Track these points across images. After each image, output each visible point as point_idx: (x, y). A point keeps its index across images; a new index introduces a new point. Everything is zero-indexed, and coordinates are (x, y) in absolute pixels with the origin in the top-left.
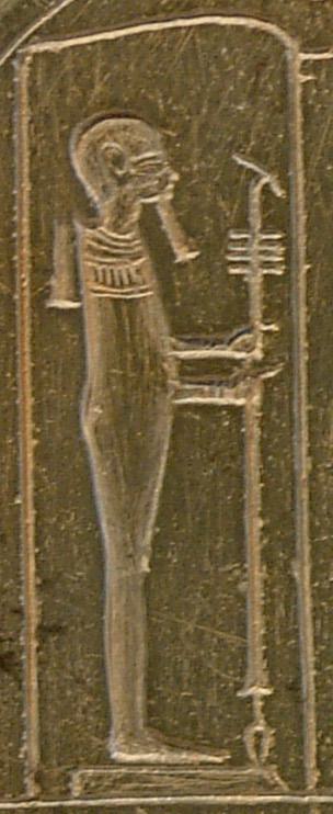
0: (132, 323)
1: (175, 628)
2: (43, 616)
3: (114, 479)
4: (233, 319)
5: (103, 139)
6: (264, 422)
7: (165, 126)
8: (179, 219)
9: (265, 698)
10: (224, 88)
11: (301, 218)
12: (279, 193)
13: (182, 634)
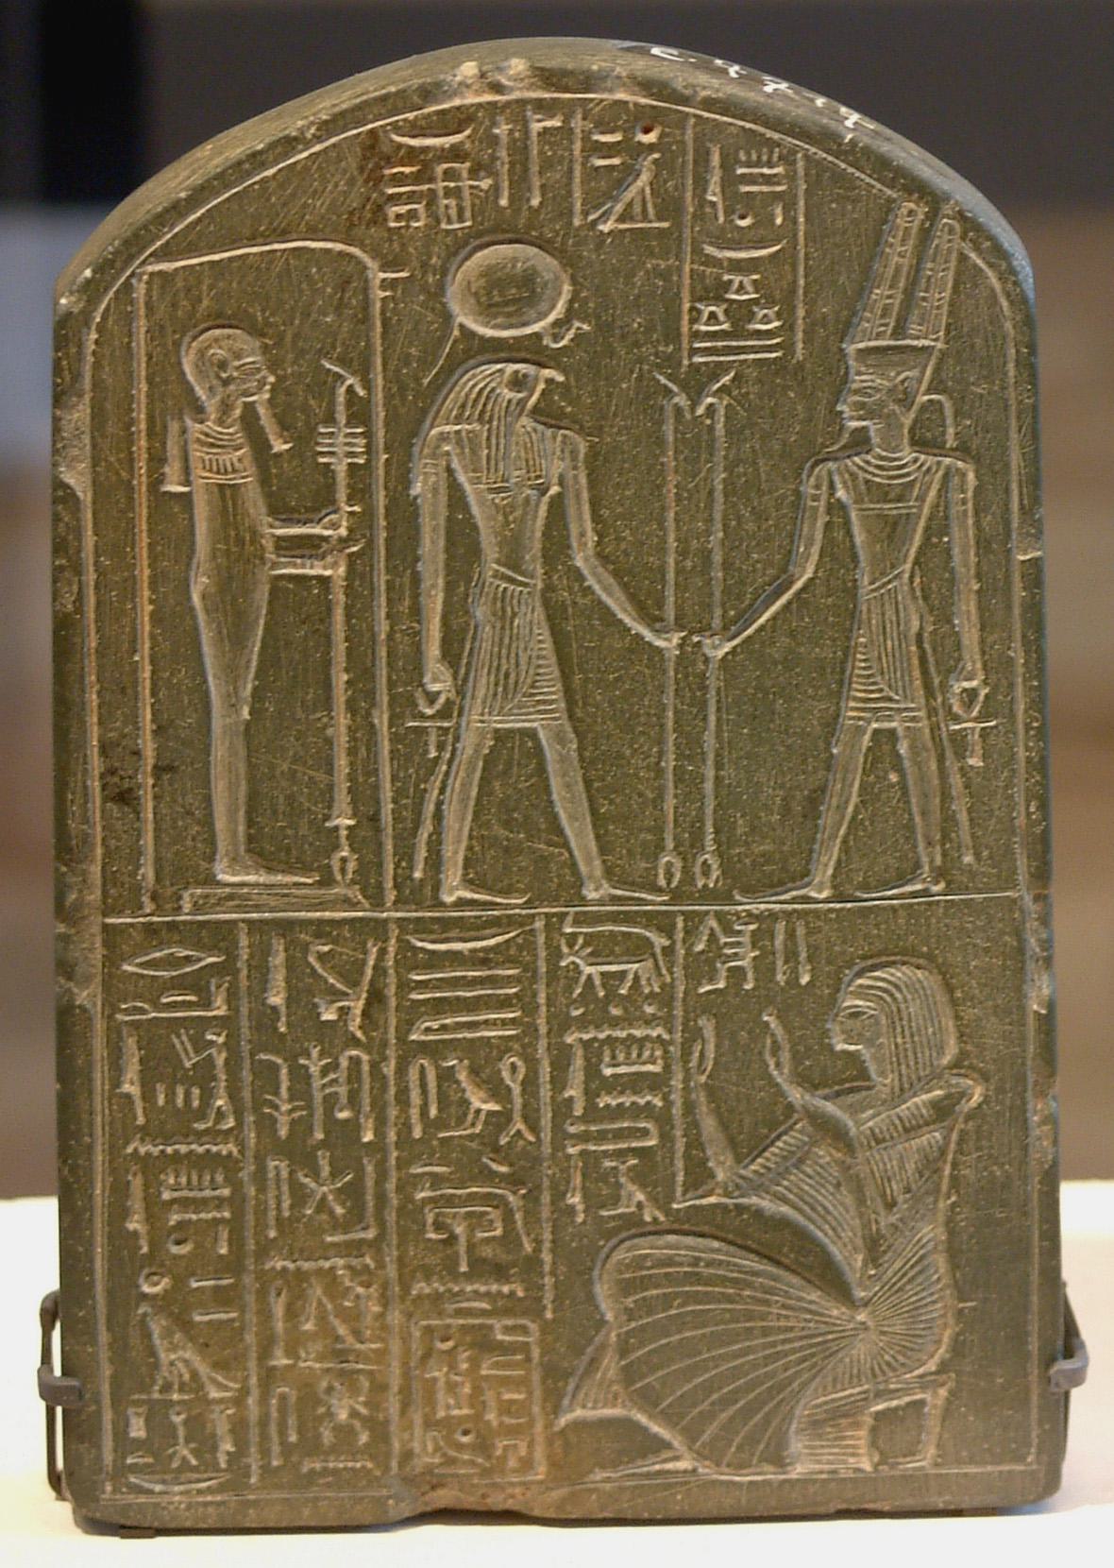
0: (235, 505)
1: (272, 767)
2: (158, 757)
3: (219, 639)
5: (210, 346)
6: (349, 590)
7: (263, 335)
8: (275, 415)
9: (349, 828)
10: (314, 303)
11: (380, 414)
12: (361, 393)
13: (278, 773)
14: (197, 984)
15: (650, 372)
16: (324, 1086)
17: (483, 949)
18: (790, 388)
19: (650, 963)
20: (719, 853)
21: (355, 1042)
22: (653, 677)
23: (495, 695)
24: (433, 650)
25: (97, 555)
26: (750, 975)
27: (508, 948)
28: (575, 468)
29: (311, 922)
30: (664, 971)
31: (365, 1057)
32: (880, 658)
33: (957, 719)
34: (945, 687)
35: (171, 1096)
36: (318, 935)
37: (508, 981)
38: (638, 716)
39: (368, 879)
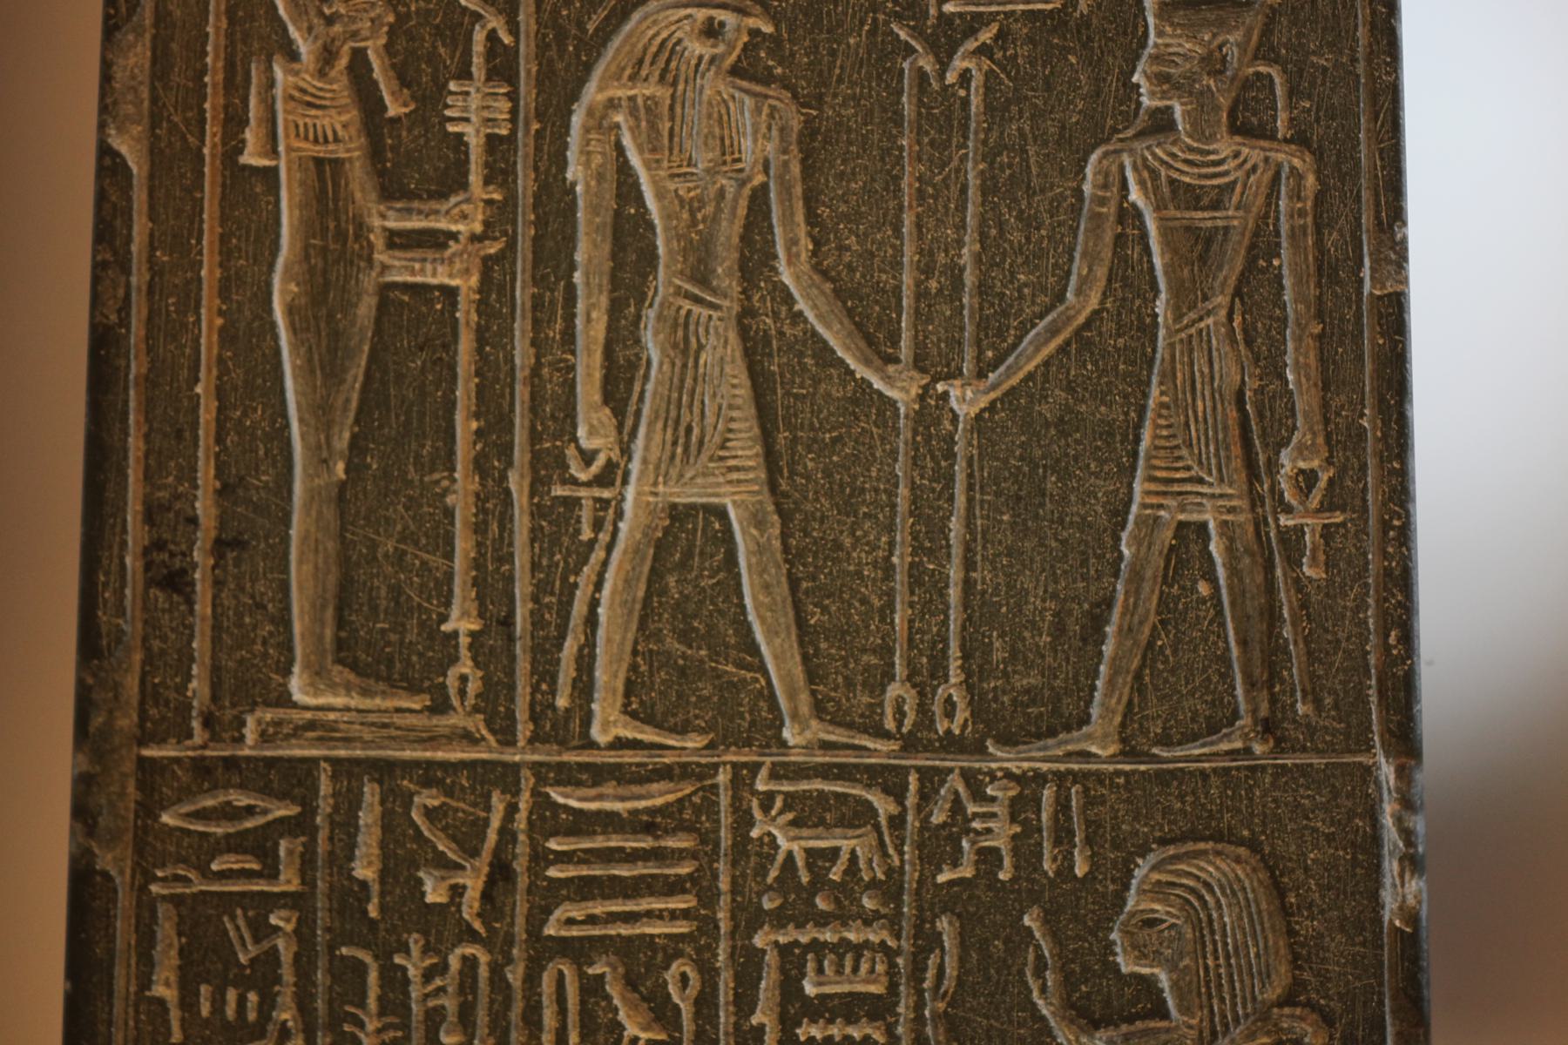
1: (374, 546)
3: (306, 371)
4: (452, 181)
6: (483, 306)
8: (393, 66)
9: (472, 634)
11: (527, 68)
14: (260, 845)
15: (887, 23)
16: (427, 996)
17: (647, 811)
18: (1069, 50)
19: (872, 839)
20: (968, 685)
21: (472, 936)
22: (882, 439)
23: (673, 457)
24: (588, 390)
25: (152, 247)
26: (1007, 862)
27: (680, 812)
28: (785, 151)
29: (417, 763)
30: (891, 851)
31: (484, 958)
32: (1187, 425)
33: (1288, 510)
34: (1273, 466)
35: (218, 1003)
36: (427, 783)
37: (679, 855)
38: (863, 490)
39: (494, 706)
